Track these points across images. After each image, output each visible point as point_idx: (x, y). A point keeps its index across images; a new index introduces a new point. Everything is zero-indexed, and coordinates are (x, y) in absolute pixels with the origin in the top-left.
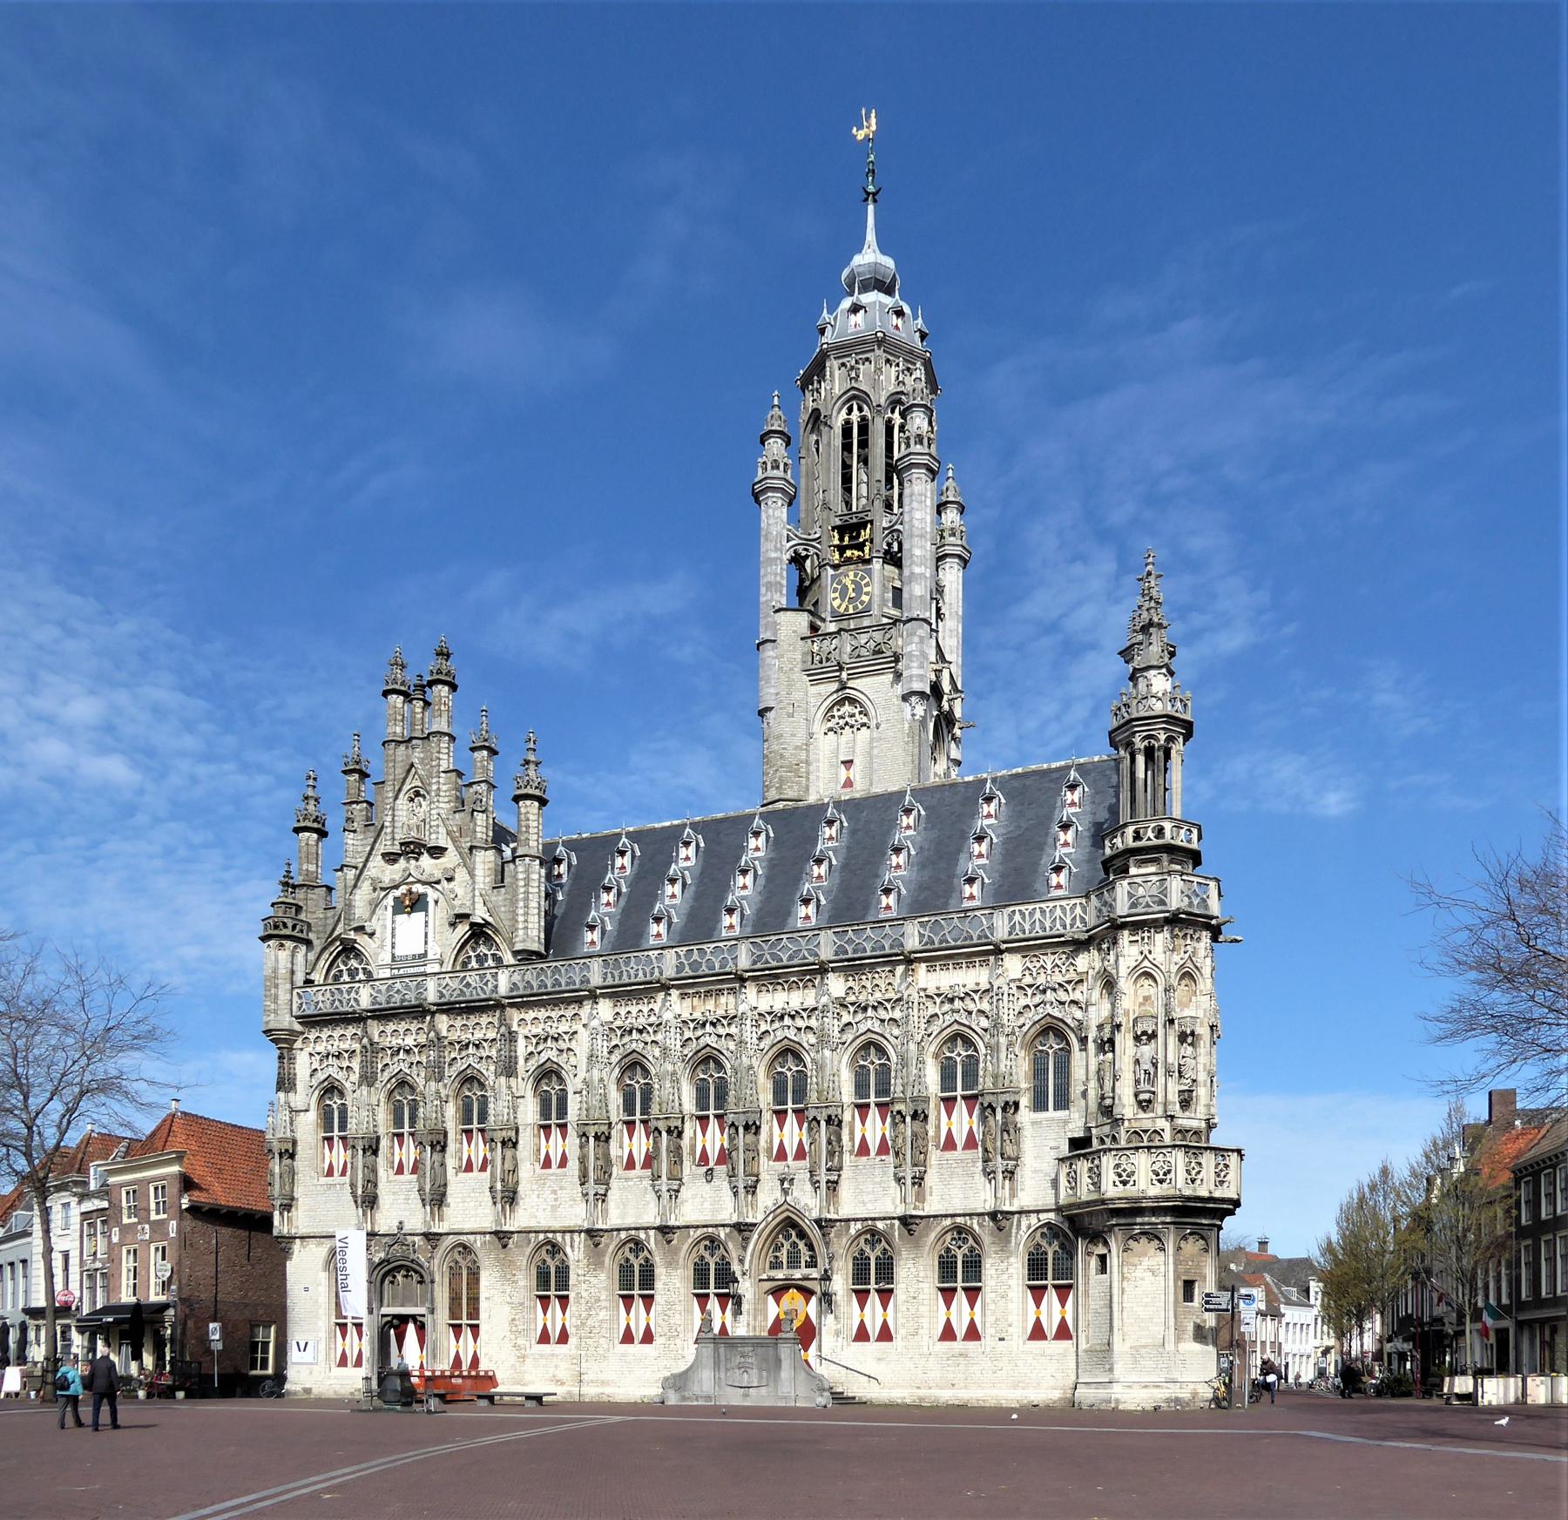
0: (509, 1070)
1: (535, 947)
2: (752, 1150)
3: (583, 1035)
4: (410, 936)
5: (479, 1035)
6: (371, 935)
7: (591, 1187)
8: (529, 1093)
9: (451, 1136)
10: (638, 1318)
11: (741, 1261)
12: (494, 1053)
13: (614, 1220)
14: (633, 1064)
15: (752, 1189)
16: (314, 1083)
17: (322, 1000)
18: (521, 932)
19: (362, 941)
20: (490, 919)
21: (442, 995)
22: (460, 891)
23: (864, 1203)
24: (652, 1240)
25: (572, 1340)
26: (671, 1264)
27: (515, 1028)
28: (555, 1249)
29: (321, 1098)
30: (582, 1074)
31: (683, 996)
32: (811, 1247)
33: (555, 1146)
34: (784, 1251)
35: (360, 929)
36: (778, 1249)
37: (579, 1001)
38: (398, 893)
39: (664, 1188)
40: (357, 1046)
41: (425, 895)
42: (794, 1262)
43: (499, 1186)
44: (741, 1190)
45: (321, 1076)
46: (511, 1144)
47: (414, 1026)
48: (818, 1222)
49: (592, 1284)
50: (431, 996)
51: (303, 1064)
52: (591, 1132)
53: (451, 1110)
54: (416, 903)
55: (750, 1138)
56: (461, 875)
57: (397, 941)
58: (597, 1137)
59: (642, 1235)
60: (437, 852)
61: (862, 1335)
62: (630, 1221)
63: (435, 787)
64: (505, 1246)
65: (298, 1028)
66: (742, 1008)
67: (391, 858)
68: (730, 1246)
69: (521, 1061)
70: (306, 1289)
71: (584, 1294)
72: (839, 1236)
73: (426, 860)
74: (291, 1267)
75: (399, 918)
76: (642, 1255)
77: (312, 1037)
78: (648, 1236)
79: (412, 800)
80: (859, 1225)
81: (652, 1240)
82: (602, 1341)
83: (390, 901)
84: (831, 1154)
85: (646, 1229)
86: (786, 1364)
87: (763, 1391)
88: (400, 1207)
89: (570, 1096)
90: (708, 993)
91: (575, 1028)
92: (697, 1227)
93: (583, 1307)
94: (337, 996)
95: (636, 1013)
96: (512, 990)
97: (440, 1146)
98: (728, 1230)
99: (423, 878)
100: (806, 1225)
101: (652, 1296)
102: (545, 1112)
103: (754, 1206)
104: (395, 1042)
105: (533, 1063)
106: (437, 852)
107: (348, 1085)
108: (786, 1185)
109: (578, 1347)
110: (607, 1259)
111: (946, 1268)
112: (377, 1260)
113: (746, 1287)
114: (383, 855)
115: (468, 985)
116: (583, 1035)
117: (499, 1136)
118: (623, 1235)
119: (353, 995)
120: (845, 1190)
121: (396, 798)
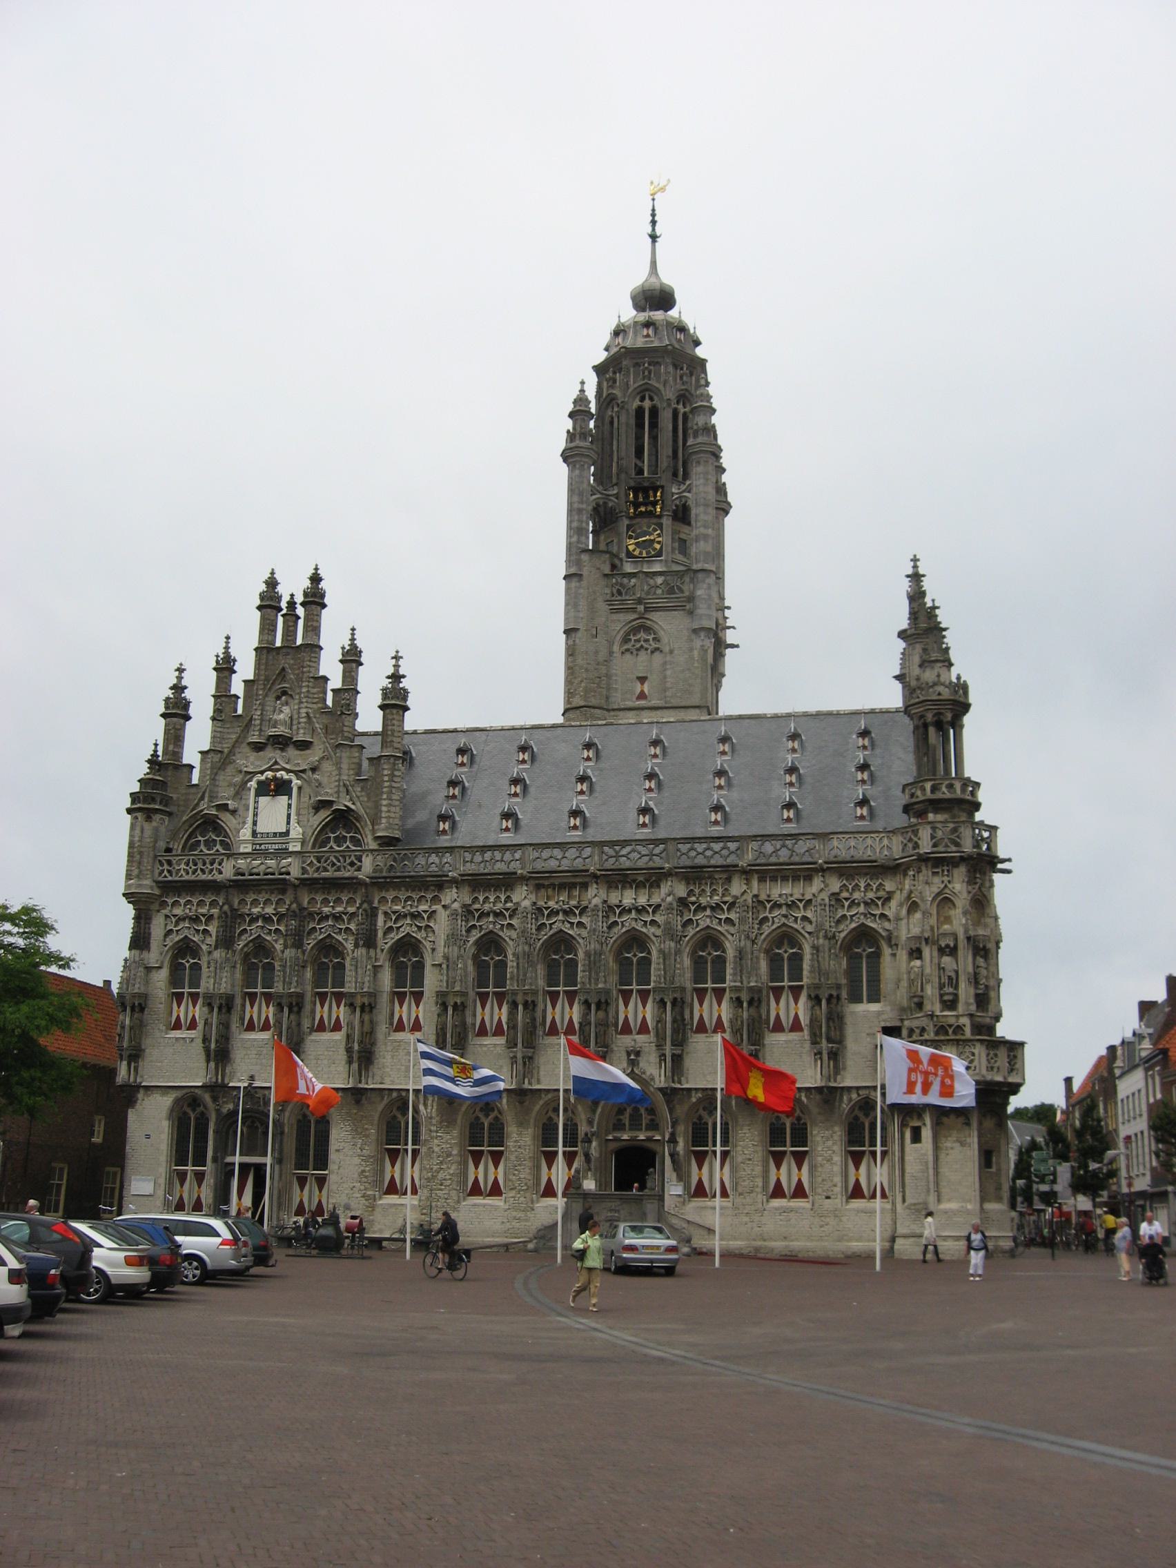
0: (369, 941)
1: (397, 834)
2: (604, 1025)
3: (443, 915)
4: (273, 815)
5: (339, 909)
6: (234, 812)
8: (387, 964)
9: (308, 997)
10: (484, 1173)
12: (353, 927)
14: (490, 943)
16: (169, 942)
17: (183, 872)
18: (384, 821)
20: (353, 807)
21: (304, 871)
22: (325, 780)
24: (505, 1101)
26: (521, 1124)
27: (376, 904)
29: (175, 958)
30: (441, 950)
31: (538, 887)
32: (652, 1111)
33: (405, 1012)
34: (627, 1115)
35: (224, 807)
36: (621, 1111)
37: (440, 886)
38: (263, 778)
39: (519, 1055)
40: (215, 911)
41: (290, 781)
42: (635, 1125)
43: (356, 1047)
45: (176, 938)
46: (369, 1008)
47: (274, 899)
48: (661, 1090)
50: (295, 872)
51: (158, 927)
52: (451, 1000)
53: (309, 974)
54: (281, 788)
55: (601, 1014)
56: (327, 766)
57: (259, 819)
58: (455, 1006)
60: (304, 745)
63: (304, 690)
64: (358, 1102)
65: (157, 892)
66: (596, 901)
67: (258, 747)
69: (380, 934)
70: (148, 1137)
71: (436, 1149)
73: (292, 752)
74: (132, 1115)
75: (262, 799)
76: (492, 1115)
77: (170, 901)
79: (278, 698)
83: (253, 784)
84: (675, 1031)
88: (253, 1063)
89: (428, 970)
90: (562, 887)
91: (434, 907)
94: (200, 865)
95: (492, 901)
96: (375, 871)
97: (295, 1005)
99: (287, 766)
102: (399, 980)
104: (255, 910)
105: (395, 937)
106: (304, 745)
107: (204, 947)
109: (428, 1198)
111: (776, 1135)
112: (225, 1111)
114: (249, 744)
115: (334, 864)
116: (443, 915)
117: (358, 1001)
119: (216, 865)
120: (689, 1063)
121: (266, 695)
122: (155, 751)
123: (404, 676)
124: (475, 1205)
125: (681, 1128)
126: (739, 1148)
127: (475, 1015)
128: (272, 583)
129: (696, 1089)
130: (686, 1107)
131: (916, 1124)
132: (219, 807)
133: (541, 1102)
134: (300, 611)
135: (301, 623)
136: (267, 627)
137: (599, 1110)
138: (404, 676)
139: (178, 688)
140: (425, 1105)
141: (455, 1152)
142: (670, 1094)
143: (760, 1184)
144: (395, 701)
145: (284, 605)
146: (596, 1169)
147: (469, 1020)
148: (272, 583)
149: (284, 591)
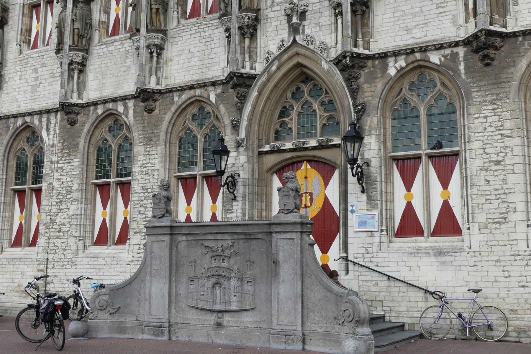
7: (68, 55)
11: (236, 127)
13: (92, 94)
15: (250, 31)
23: (408, 30)
24: (131, 112)
25: (42, 241)
26: (149, 141)
28: (32, 135)
32: (329, 105)
36: (284, 112)
44: (235, 31)
48: (337, 62)
49: (65, 172)
59: (121, 108)
61: (410, 226)
62: (108, 93)
68: (222, 109)
71: (56, 185)
72: (372, 79)
78: (126, 108)
80: (402, 62)
81: (131, 112)
82: (72, 241)
85: (124, 99)
86: (288, 271)
87: (247, 319)
92: (182, 89)
93: (54, 200)
98: (219, 90)
100: (325, 68)
101: (129, 183)
103: (252, 54)
108: (295, 20)
110: (82, 142)
113: (237, 162)
118: (100, 110)
124: (95, 257)
125: (371, 121)
126: (476, 145)
127: (107, 12)
129: (396, 54)
130: (380, 85)
133: (173, 109)
137: (248, 108)
140: (48, 129)
141: (75, 187)
142: (351, 65)
143: (521, 207)
146: (244, 198)
147: (97, 15)
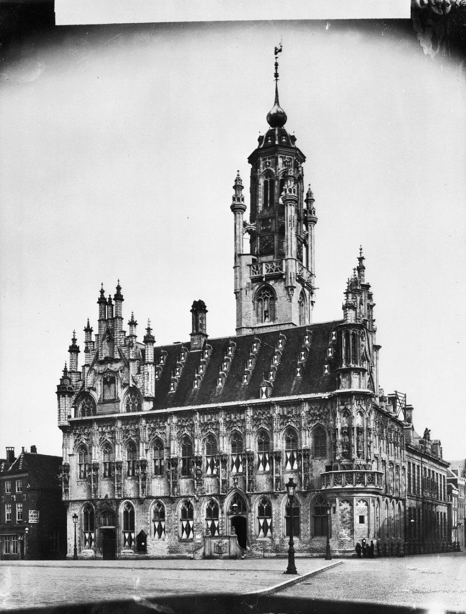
6: (95, 390)
19: (93, 393)
67: (102, 363)
121: (103, 340)
122: (66, 367)
123: (152, 329)
128: (102, 292)
131: (334, 505)
132: (89, 388)
134: (113, 302)
135: (114, 307)
136: (102, 312)
138: (152, 329)
139: (74, 340)
144: (149, 339)
145: (107, 300)
148: (102, 292)
149: (106, 296)
